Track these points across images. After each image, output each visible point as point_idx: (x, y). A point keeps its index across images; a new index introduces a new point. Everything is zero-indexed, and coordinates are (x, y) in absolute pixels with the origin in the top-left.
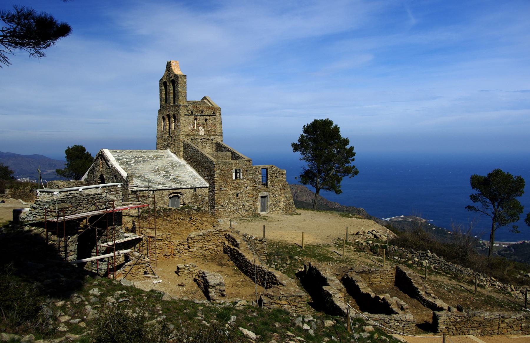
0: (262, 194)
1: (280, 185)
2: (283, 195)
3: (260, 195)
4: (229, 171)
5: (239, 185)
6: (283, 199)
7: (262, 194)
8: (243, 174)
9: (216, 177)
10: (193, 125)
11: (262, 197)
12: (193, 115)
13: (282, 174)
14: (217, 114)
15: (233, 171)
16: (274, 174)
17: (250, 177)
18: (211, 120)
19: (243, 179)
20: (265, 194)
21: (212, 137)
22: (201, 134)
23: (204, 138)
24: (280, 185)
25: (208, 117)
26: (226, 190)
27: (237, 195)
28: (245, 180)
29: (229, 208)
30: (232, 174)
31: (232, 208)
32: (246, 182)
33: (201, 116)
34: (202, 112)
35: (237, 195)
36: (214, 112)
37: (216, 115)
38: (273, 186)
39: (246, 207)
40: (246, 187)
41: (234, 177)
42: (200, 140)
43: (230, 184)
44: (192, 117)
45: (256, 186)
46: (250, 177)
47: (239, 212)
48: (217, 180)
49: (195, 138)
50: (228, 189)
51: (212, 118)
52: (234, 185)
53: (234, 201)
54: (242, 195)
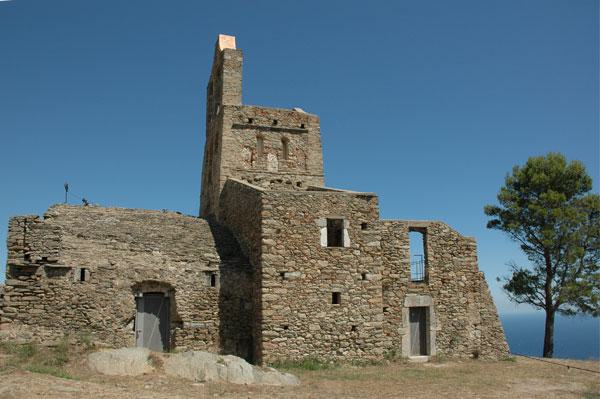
0: (413, 300)
1: (464, 278)
2: (471, 306)
3: (408, 303)
4: (310, 222)
5: (339, 264)
6: (473, 320)
7: (413, 300)
8: (352, 237)
9: (266, 238)
10: (251, 149)
11: (412, 310)
12: (252, 128)
13: (469, 249)
14: (310, 129)
15: (322, 222)
16: (446, 245)
17: (372, 244)
18: (294, 141)
19: (352, 249)
20: (422, 301)
21: (299, 179)
22: (270, 169)
23: (279, 177)
24: (464, 278)
25: (289, 135)
26: (297, 279)
27: (336, 298)
28: (358, 253)
29: (309, 335)
30: (317, 231)
31: (318, 336)
32: (363, 259)
33: (272, 130)
34: (275, 122)
35: (336, 298)
36: (303, 126)
37: (307, 132)
38: (443, 281)
39: (363, 334)
40: (364, 275)
41: (324, 241)
42: (268, 183)
43: (312, 261)
44: (251, 133)
45: (397, 276)
46: (372, 244)
47: (341, 350)
48: (269, 247)
49: (257, 177)
50: (304, 276)
51: (297, 137)
52: (324, 264)
53: (323, 314)
54: (348, 298)
